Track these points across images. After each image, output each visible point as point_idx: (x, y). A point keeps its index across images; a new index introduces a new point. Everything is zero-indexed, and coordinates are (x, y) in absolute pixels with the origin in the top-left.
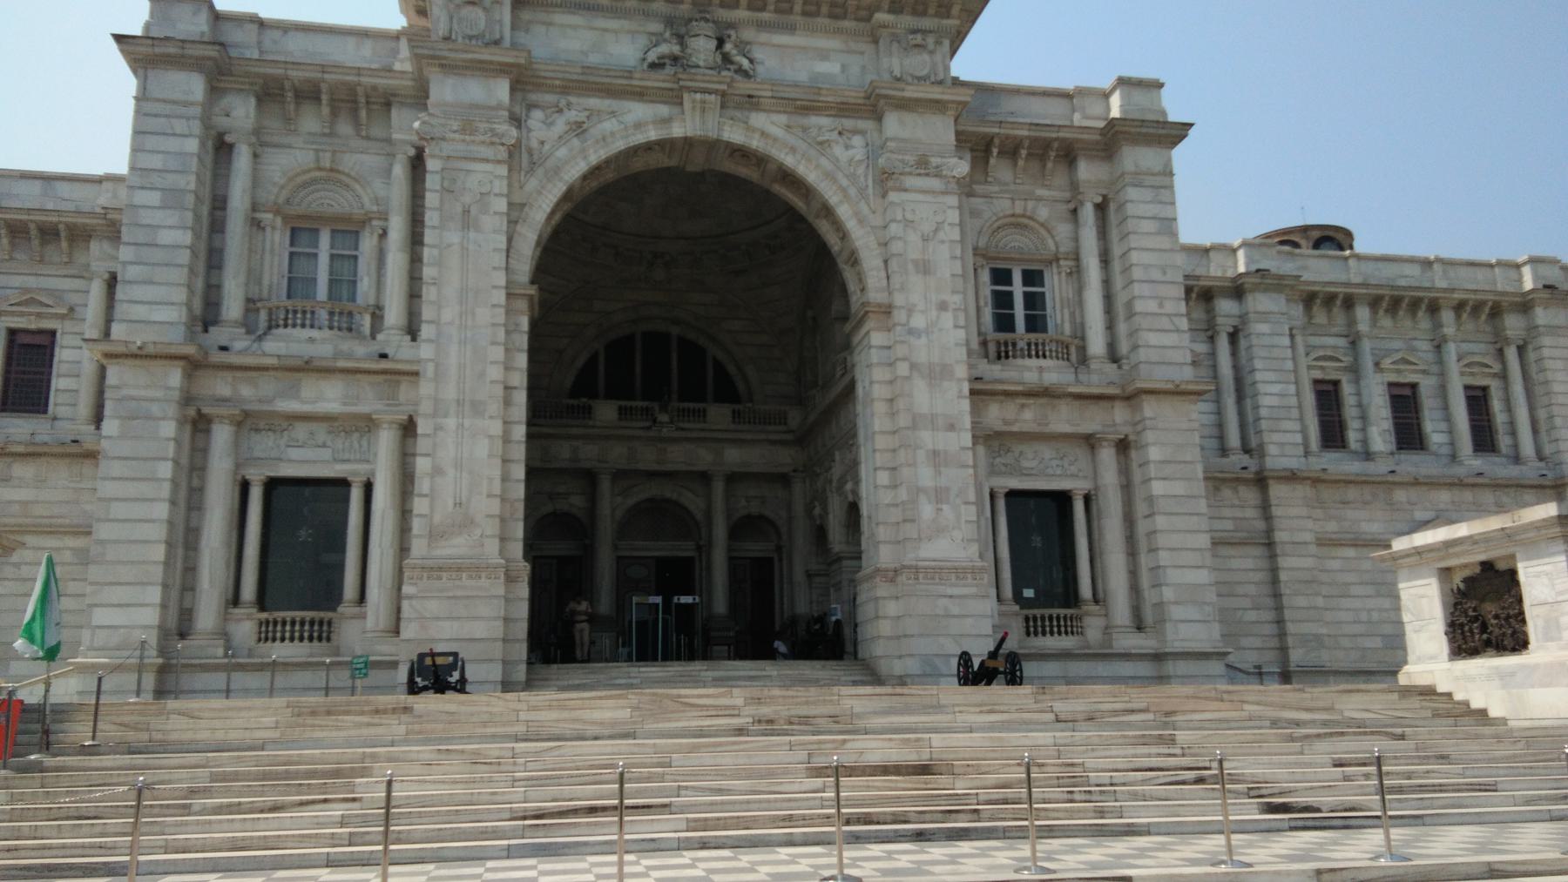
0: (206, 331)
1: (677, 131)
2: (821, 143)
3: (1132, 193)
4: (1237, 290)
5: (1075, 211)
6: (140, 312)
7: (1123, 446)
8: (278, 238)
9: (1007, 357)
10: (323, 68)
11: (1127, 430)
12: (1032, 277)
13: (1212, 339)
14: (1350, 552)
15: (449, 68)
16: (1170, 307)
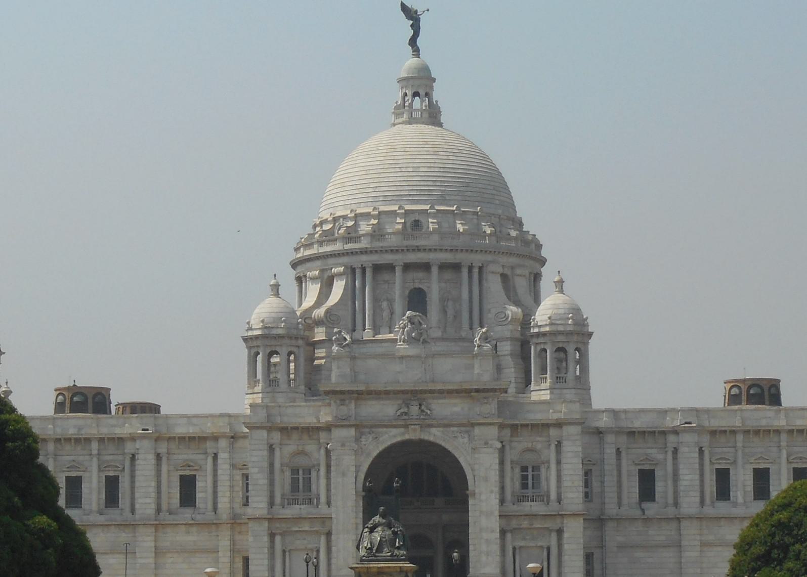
0: (272, 508)
1: (407, 437)
2: (454, 437)
3: (565, 443)
4: (675, 432)
5: (550, 445)
6: (255, 505)
7: (560, 532)
8: (288, 474)
9: (521, 501)
10: (300, 424)
11: (560, 525)
12: (534, 469)
13: (666, 452)
14: (720, 549)
15: (336, 426)
16: (576, 484)
